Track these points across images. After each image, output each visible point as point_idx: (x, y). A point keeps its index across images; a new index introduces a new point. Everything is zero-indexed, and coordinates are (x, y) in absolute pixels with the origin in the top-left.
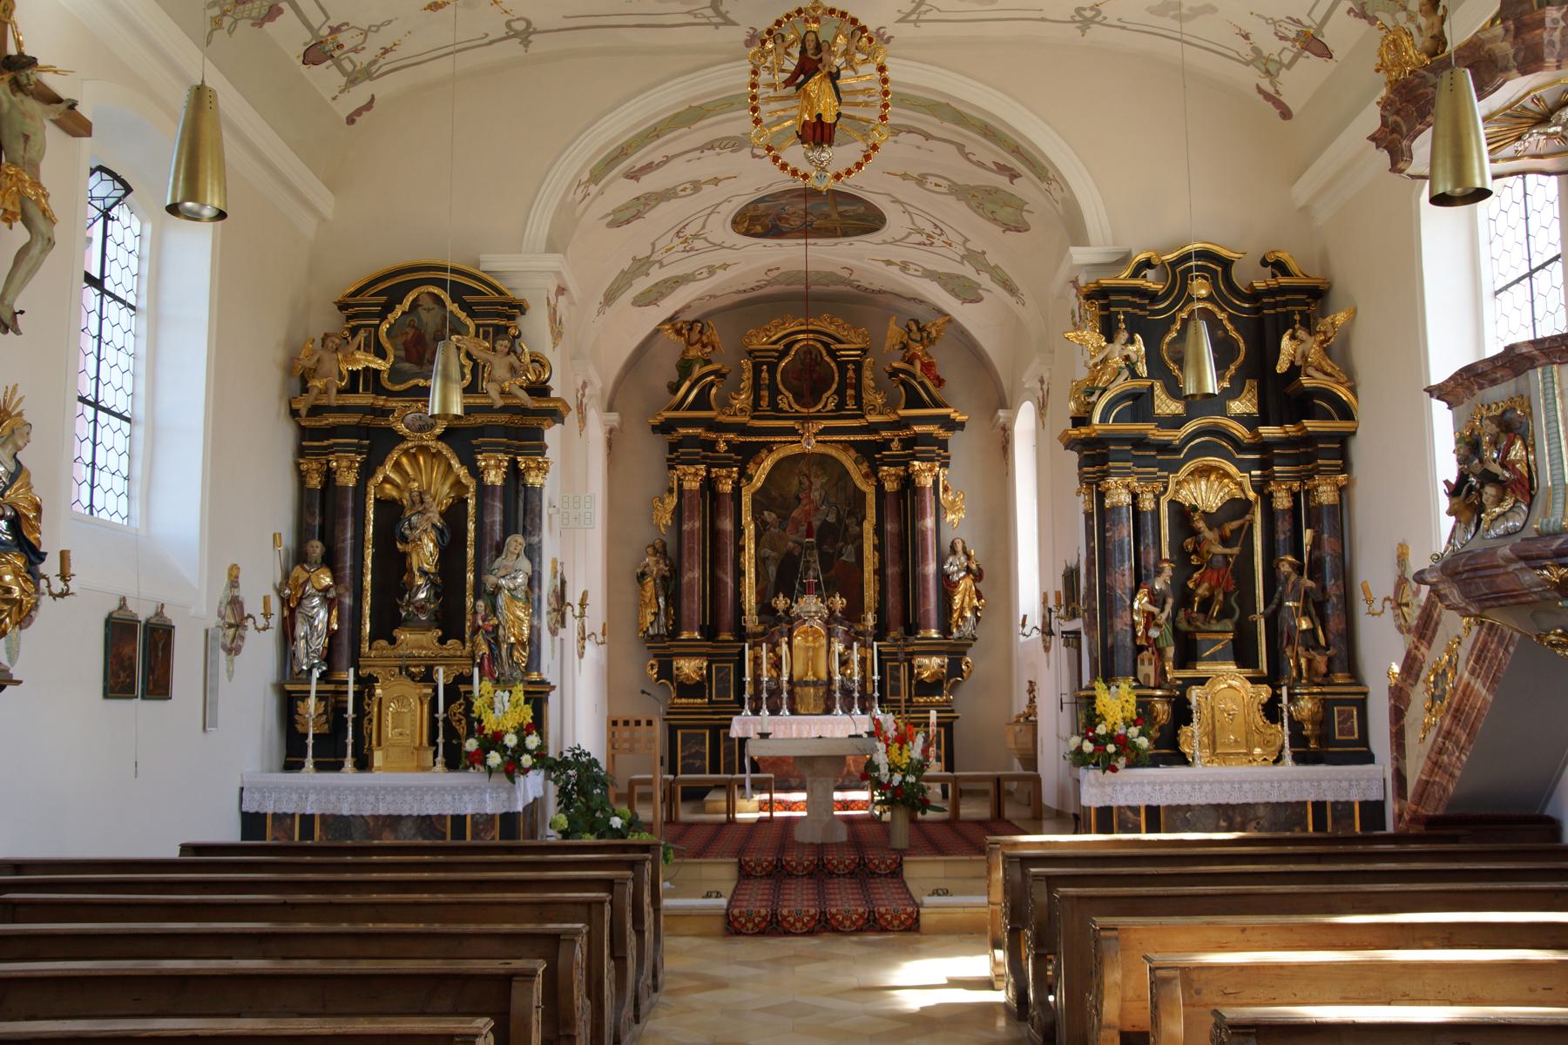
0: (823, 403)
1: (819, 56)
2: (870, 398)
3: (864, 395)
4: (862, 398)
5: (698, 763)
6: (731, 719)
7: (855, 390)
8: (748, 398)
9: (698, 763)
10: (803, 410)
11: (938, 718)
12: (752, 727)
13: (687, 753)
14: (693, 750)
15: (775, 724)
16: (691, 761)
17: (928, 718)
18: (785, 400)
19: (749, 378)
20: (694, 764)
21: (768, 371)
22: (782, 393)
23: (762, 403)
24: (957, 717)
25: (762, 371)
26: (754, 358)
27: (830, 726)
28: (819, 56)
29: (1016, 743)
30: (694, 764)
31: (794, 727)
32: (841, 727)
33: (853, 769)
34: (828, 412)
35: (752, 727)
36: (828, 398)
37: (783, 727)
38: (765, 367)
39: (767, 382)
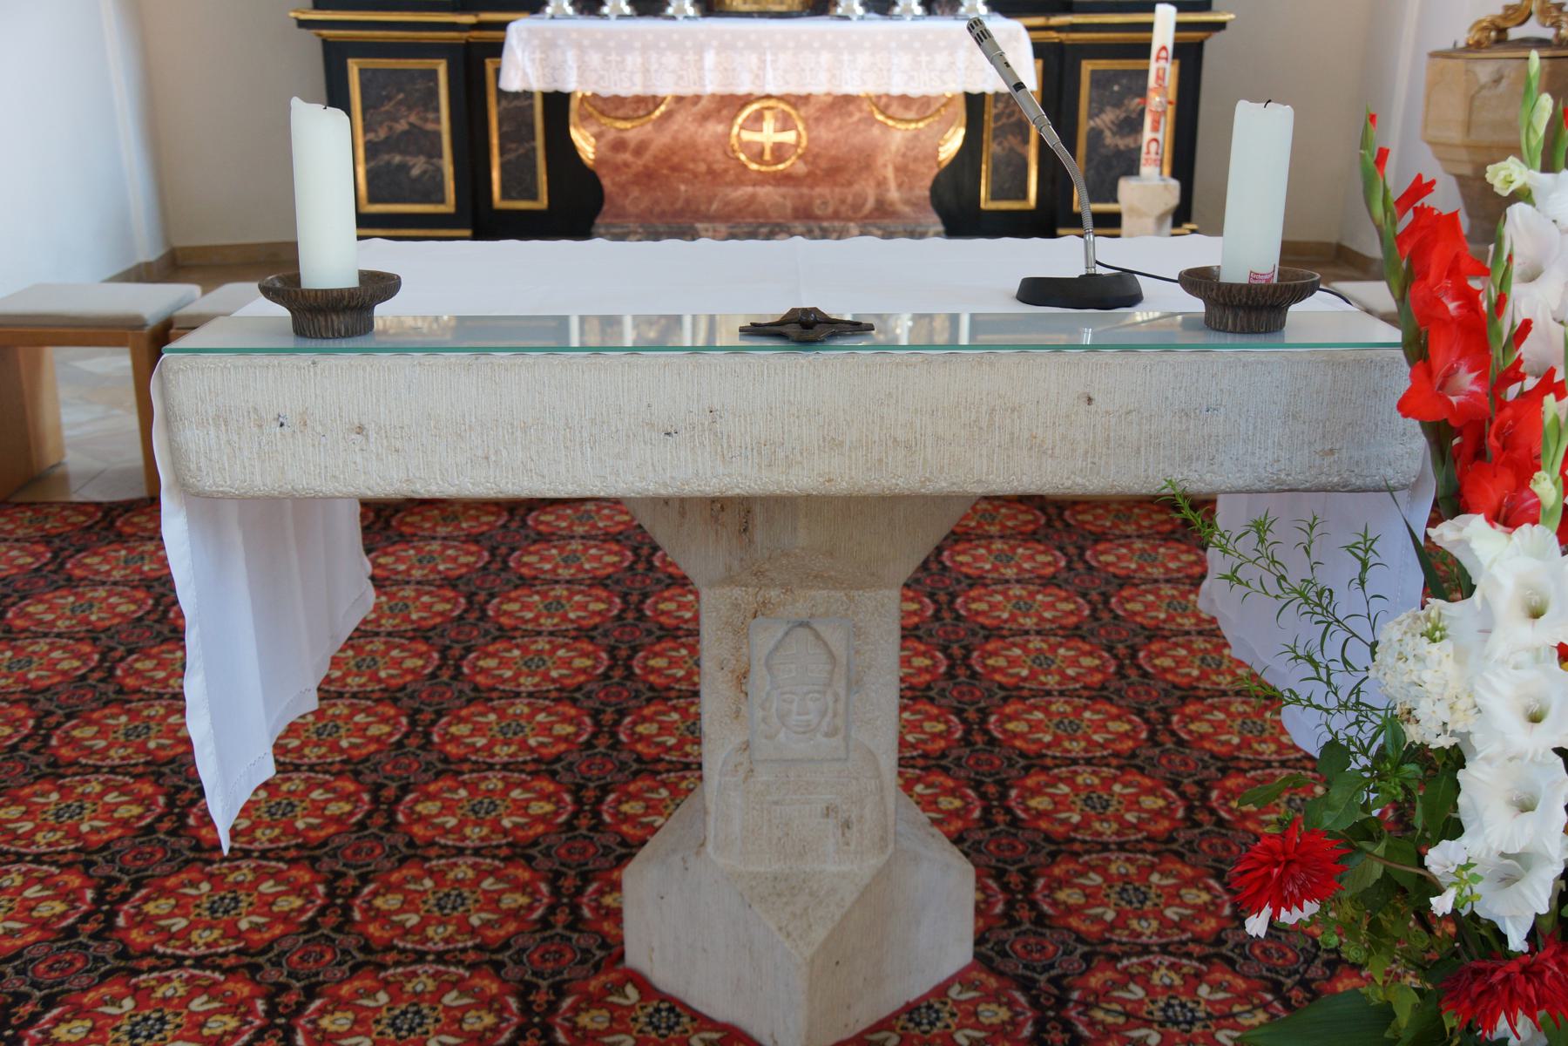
5: (418, 166)
6: (503, 26)
9: (418, 166)
11: (1180, 27)
12: (571, 56)
13: (382, 134)
14: (402, 126)
15: (645, 49)
16: (397, 159)
17: (1149, 27)
20: (403, 168)
24: (1220, 26)
27: (825, 57)
29: (1468, 126)
30: (403, 168)
31: (710, 58)
32: (863, 59)
33: (894, 194)
35: (571, 56)
37: (671, 60)
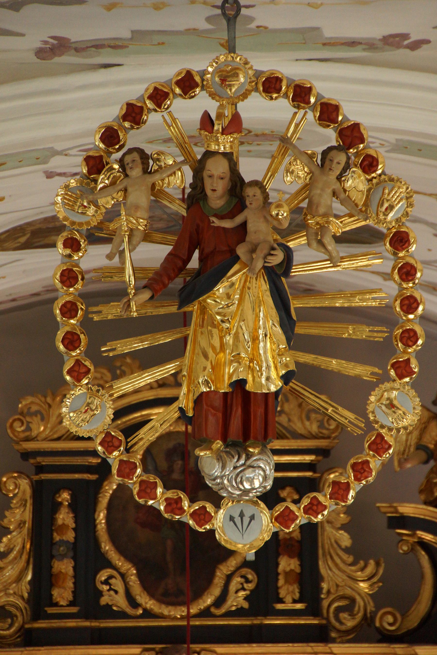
0: (216, 591)
1: (239, 219)
2: (340, 578)
3: (323, 570)
4: (318, 578)
7: (300, 557)
8: (19, 579)
10: (166, 610)
18: (118, 584)
19: (21, 524)
21: (73, 506)
22: (109, 565)
23: (55, 593)
25: (57, 506)
26: (40, 469)
28: (239, 219)
34: (229, 614)
36: (229, 578)
38: (65, 496)
39: (70, 536)
